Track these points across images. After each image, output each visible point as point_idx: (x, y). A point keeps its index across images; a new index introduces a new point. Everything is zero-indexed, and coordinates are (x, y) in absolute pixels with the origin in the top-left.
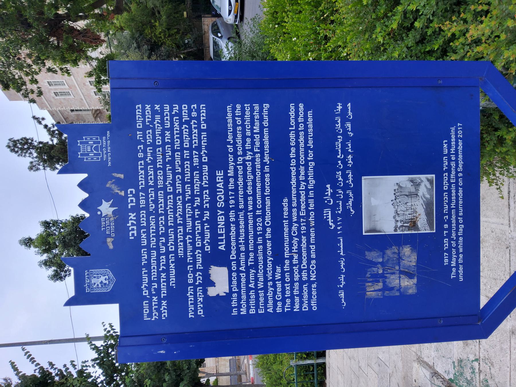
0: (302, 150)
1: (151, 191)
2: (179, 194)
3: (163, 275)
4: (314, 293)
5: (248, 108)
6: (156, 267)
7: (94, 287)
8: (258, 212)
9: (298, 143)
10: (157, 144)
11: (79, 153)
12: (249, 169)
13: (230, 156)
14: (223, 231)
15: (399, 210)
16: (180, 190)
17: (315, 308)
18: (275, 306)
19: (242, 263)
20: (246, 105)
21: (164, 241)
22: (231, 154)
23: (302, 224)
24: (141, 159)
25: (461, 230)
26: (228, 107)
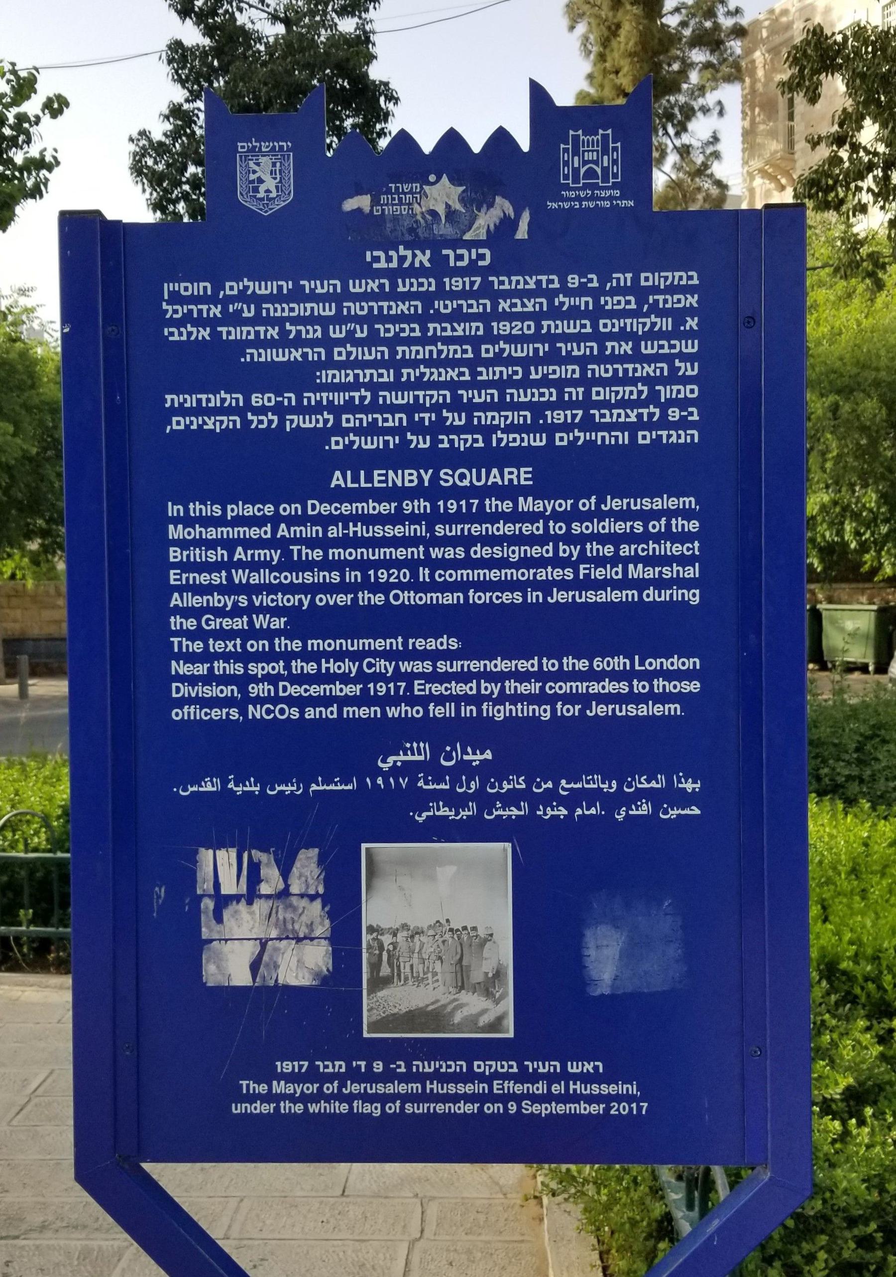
0: (582, 687)
1: (485, 305)
2: (474, 374)
3: (273, 332)
4: (216, 714)
5: (688, 549)
6: (295, 314)
7: (251, 164)
8: (424, 574)
9: (599, 676)
10: (602, 322)
11: (580, 132)
12: (535, 551)
13: (570, 502)
14: (380, 482)
15: (424, 939)
16: (484, 377)
17: (177, 715)
18: (186, 612)
19: (298, 529)
20: (696, 544)
21: (359, 335)
22: (575, 506)
23: (391, 685)
24: (563, 281)
25: (367, 1108)
26: (692, 499)
